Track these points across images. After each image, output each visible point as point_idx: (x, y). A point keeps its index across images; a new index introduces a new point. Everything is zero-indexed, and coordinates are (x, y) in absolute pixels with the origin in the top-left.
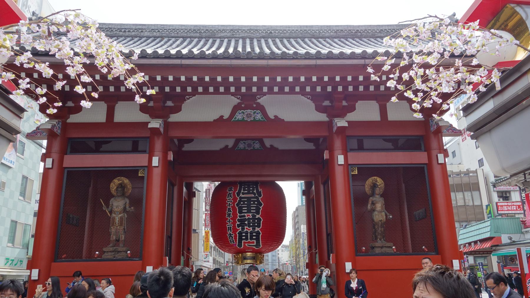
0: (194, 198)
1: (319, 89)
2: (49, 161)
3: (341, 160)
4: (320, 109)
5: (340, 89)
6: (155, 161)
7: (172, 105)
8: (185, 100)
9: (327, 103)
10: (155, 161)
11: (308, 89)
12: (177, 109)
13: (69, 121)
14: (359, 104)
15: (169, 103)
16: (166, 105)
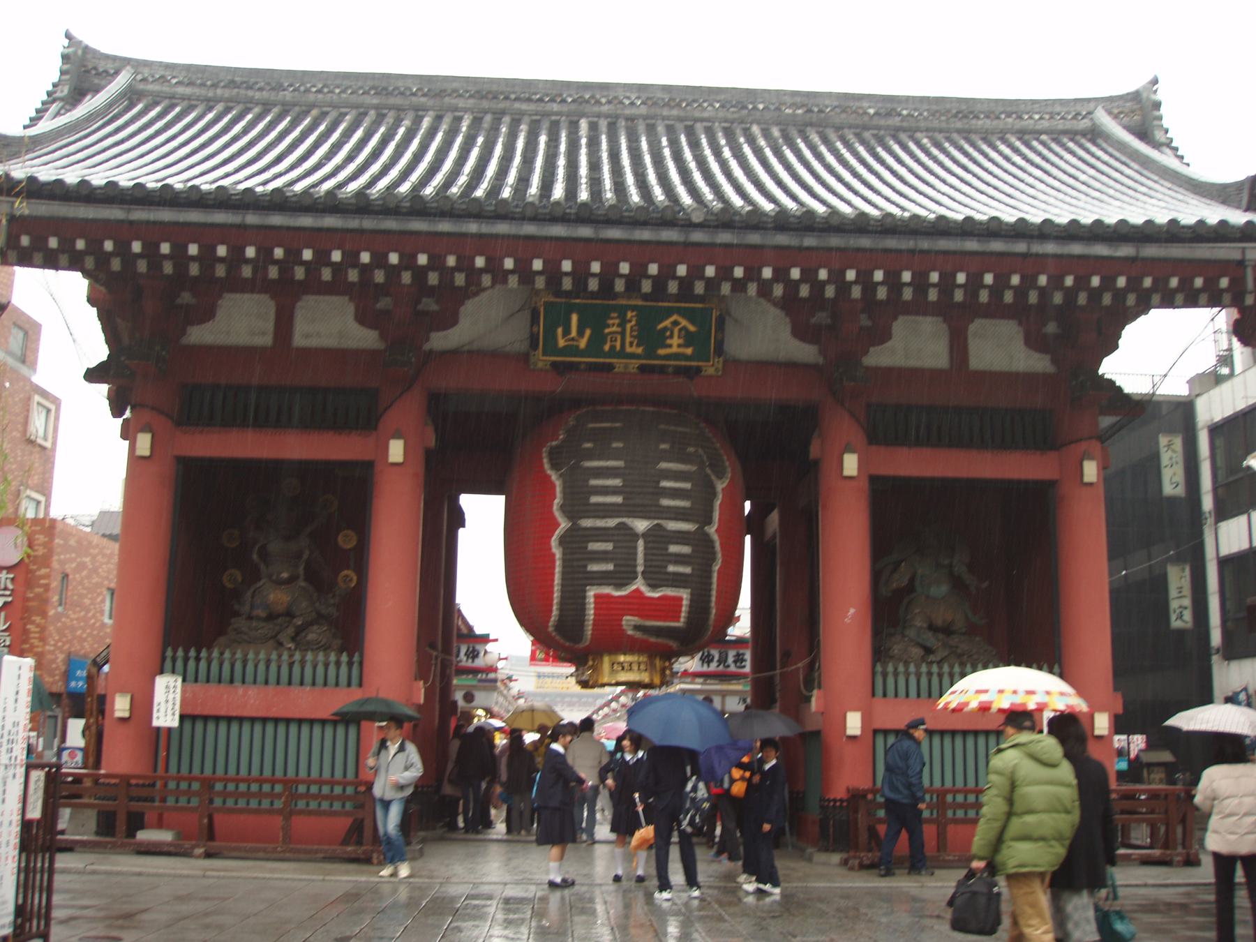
0: (461, 531)
1: (804, 291)
2: (144, 442)
3: (851, 464)
4: (802, 332)
5: (856, 292)
6: (396, 451)
7: (434, 307)
8: (469, 298)
9: (821, 318)
10: (396, 451)
11: (778, 290)
12: (448, 320)
13: (185, 341)
14: (900, 327)
15: (429, 304)
16: (420, 307)
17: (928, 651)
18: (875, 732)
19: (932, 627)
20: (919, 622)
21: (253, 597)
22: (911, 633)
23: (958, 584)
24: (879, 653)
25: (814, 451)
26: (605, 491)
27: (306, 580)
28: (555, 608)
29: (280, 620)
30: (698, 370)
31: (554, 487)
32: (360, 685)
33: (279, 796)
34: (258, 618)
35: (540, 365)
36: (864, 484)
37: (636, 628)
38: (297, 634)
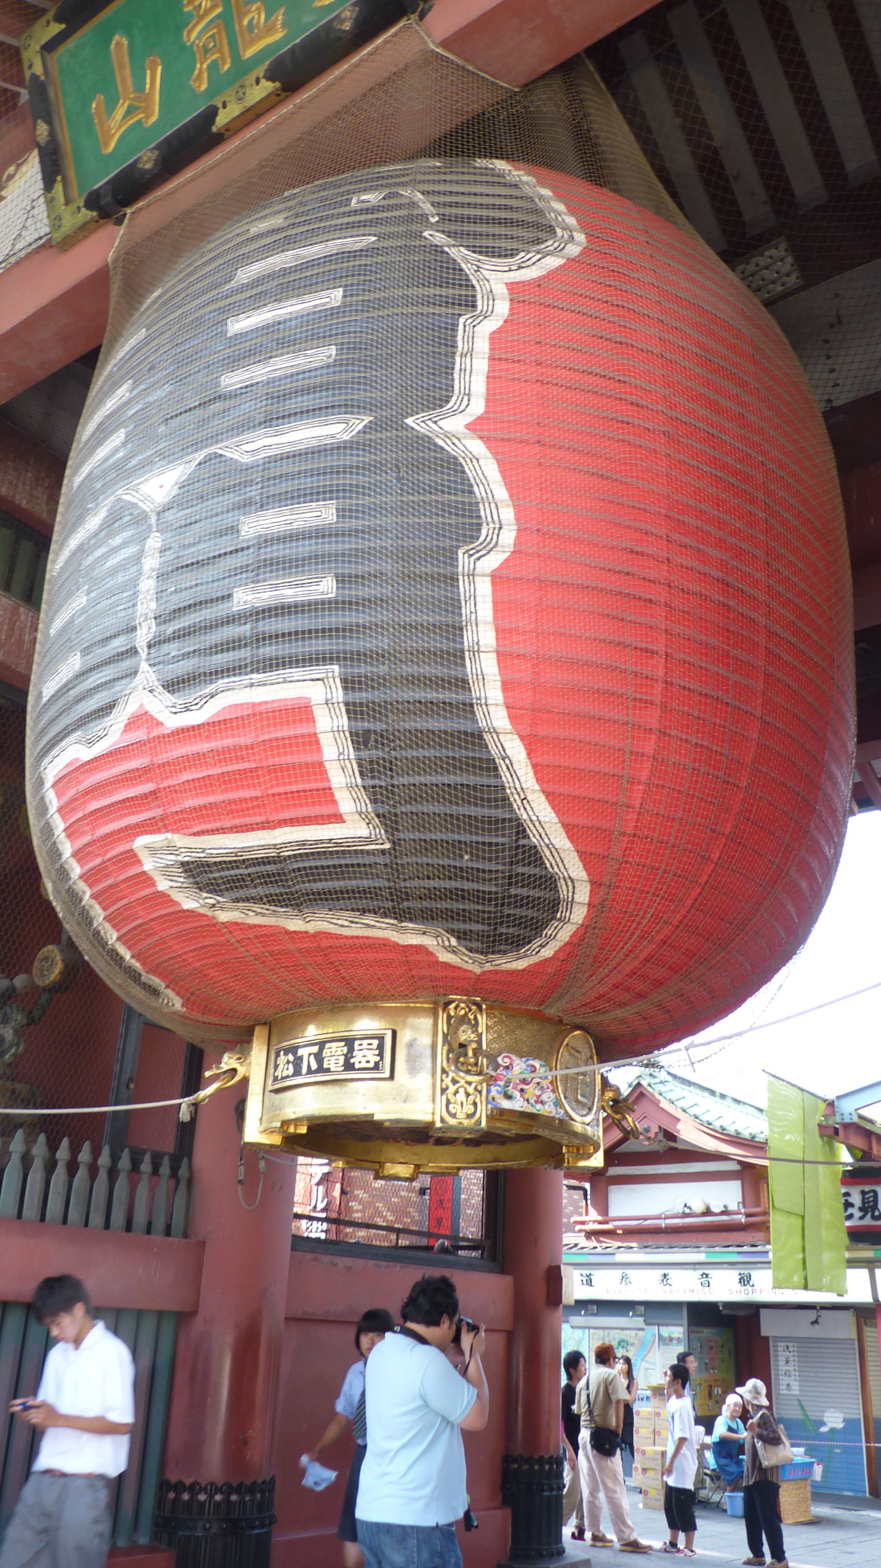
37: (199, 873)
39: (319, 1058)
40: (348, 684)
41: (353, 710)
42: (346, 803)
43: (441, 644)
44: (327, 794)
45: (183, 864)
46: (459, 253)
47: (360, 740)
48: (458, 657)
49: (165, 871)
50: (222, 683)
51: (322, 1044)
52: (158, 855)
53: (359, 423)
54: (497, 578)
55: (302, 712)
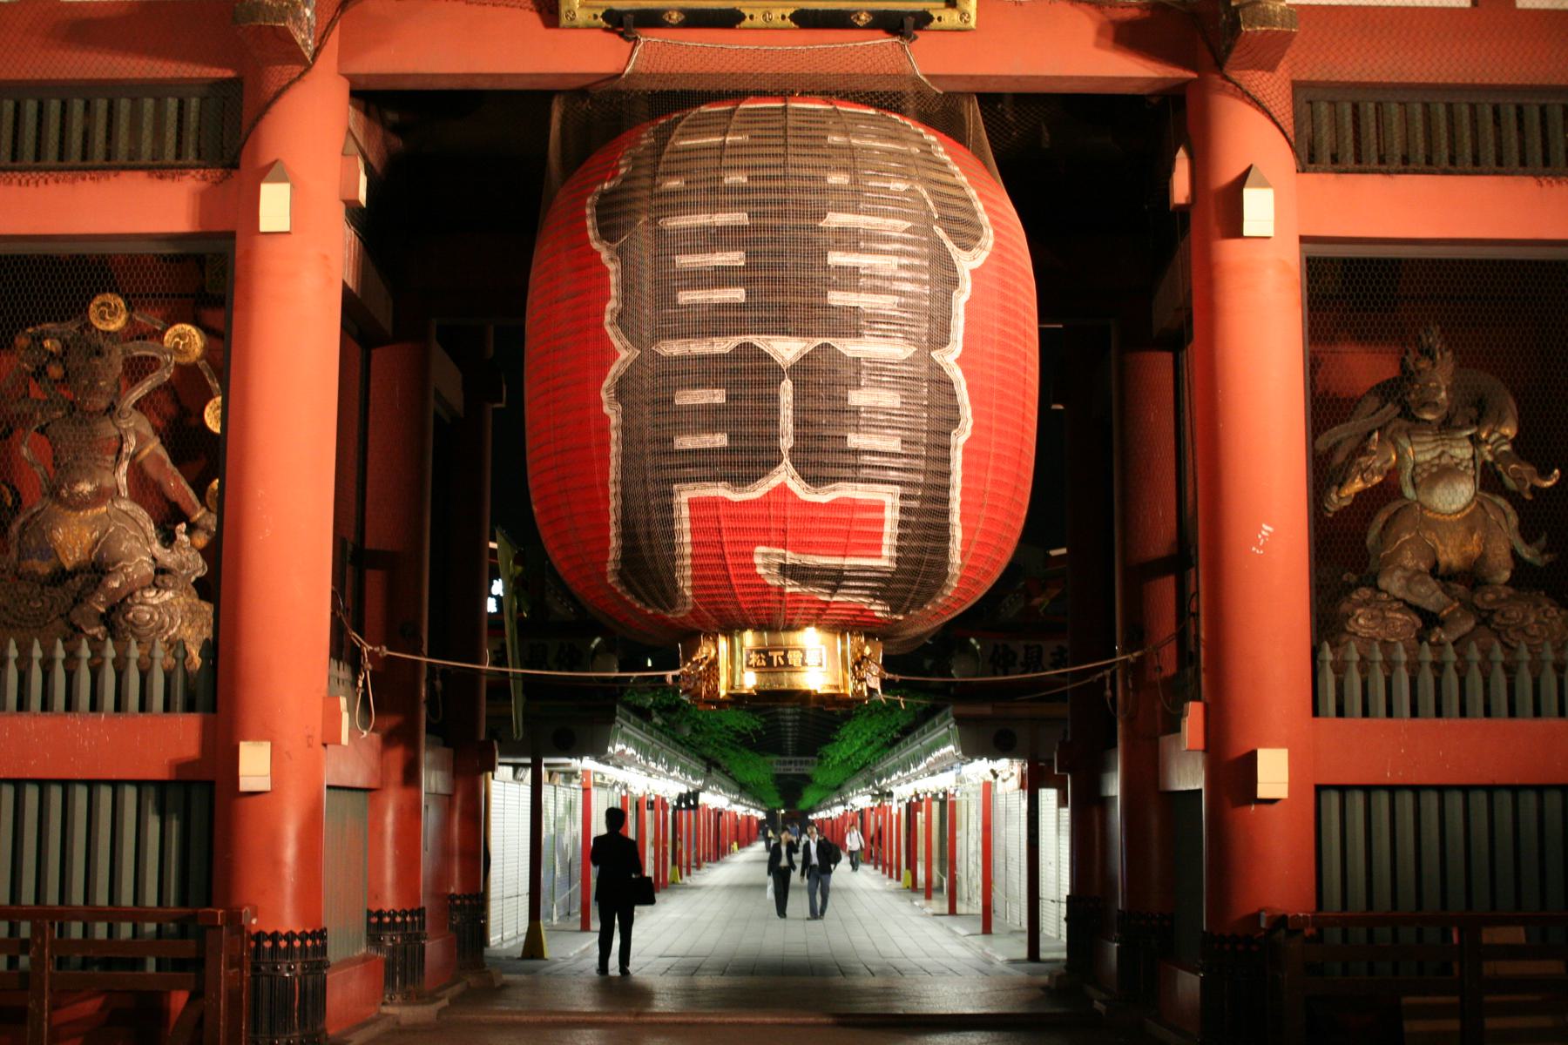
3: (1260, 210)
6: (275, 206)
17: (1430, 620)
18: (1320, 789)
19: (1434, 571)
20: (1408, 559)
21: (22, 533)
22: (1393, 583)
23: (1489, 480)
24: (1327, 624)
25: (1180, 188)
26: (722, 277)
27: (136, 497)
28: (613, 532)
29: (78, 581)
30: (923, 19)
31: (605, 272)
32: (213, 707)
33: (25, 946)
34: (33, 577)
35: (582, 16)
36: (1292, 256)
38: (112, 609)
39: (785, 658)
40: (902, 497)
41: (903, 510)
42: (885, 552)
43: (940, 481)
44: (879, 547)
45: (782, 567)
46: (950, 245)
47: (902, 524)
48: (947, 488)
49: (767, 566)
50: (840, 484)
51: (786, 652)
52: (765, 559)
53: (910, 351)
54: (966, 451)
55: (880, 508)
